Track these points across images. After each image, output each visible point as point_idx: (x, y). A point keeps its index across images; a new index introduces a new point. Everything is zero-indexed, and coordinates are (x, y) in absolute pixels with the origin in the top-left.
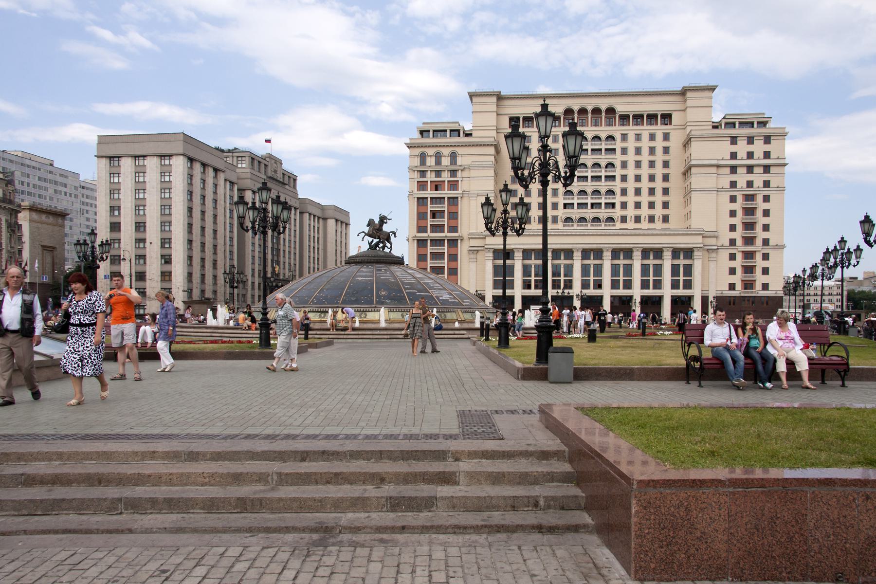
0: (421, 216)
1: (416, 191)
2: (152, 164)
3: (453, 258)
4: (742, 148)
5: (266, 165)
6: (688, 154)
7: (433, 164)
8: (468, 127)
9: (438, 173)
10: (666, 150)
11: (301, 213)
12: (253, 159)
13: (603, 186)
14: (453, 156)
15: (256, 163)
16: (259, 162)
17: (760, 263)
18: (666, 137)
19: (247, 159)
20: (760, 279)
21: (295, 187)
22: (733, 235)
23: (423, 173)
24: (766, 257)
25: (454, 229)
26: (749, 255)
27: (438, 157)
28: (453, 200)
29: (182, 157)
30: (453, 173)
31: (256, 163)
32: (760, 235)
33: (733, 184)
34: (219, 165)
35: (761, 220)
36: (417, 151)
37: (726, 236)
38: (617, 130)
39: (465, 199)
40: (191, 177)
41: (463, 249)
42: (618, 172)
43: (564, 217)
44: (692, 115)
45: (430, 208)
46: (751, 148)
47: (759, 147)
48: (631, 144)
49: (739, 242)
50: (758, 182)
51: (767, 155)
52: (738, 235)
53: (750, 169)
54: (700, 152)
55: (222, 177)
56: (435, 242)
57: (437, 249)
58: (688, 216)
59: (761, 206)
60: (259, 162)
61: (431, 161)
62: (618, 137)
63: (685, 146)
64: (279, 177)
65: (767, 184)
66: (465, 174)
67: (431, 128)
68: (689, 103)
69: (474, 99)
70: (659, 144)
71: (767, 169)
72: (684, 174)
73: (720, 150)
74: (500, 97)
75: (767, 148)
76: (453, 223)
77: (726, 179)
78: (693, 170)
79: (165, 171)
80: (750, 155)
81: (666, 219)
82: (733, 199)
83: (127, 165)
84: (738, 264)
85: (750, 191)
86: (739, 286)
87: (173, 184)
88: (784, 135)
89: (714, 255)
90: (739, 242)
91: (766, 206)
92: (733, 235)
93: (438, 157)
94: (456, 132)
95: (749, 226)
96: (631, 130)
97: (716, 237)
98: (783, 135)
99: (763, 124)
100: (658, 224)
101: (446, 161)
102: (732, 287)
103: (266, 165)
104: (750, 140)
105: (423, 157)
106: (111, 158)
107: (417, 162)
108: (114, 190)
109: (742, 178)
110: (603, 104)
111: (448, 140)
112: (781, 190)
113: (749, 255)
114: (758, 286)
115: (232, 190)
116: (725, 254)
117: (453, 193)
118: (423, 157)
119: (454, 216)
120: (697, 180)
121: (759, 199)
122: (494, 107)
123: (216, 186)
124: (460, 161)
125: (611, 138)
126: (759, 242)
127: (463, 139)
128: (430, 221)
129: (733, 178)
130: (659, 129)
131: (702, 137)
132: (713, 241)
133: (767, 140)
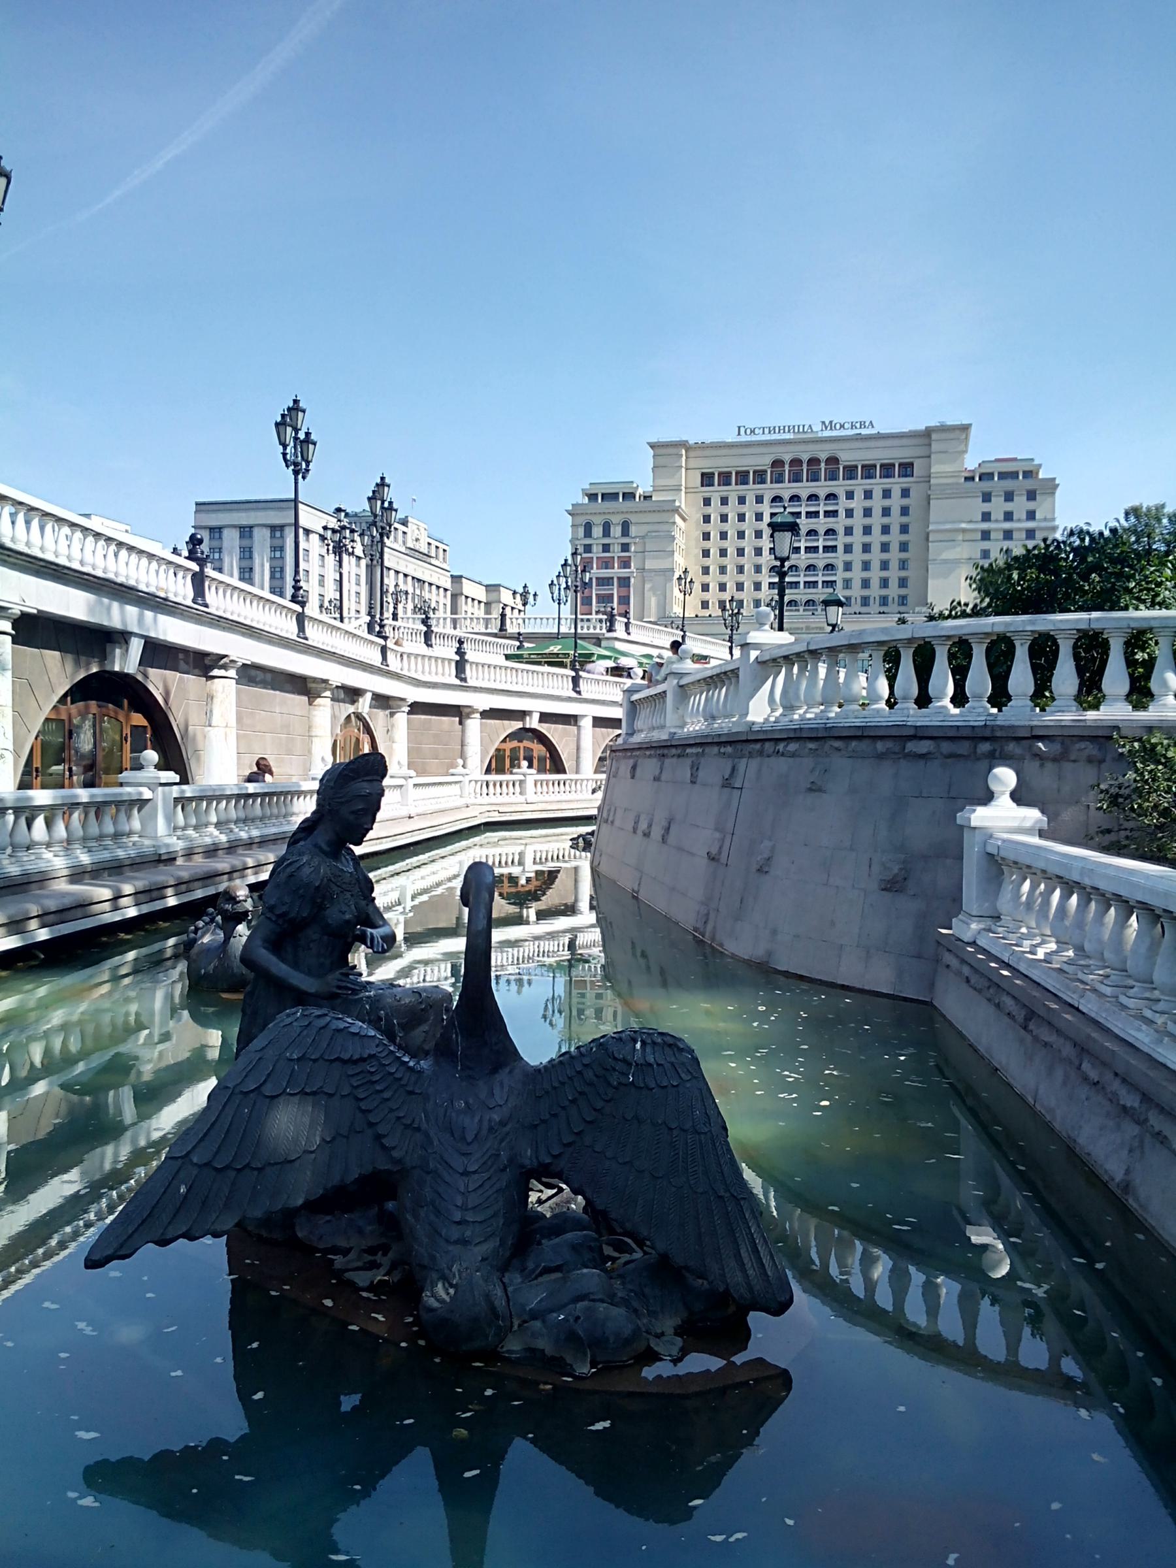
2: (261, 538)
4: (998, 506)
7: (601, 535)
9: (606, 548)
13: (821, 559)
14: (626, 527)
18: (905, 493)
27: (607, 528)
28: (625, 582)
36: (582, 520)
38: (840, 486)
42: (841, 541)
46: (1009, 506)
47: (1020, 505)
67: (599, 491)
68: (934, 447)
70: (896, 502)
80: (1008, 516)
93: (607, 528)
94: (629, 496)
96: (859, 485)
99: (1028, 474)
101: (616, 531)
103: (404, 533)
104: (1009, 497)
105: (588, 528)
107: (581, 531)
117: (624, 572)
118: (588, 528)
124: (633, 530)
130: (896, 484)
133: (1031, 496)
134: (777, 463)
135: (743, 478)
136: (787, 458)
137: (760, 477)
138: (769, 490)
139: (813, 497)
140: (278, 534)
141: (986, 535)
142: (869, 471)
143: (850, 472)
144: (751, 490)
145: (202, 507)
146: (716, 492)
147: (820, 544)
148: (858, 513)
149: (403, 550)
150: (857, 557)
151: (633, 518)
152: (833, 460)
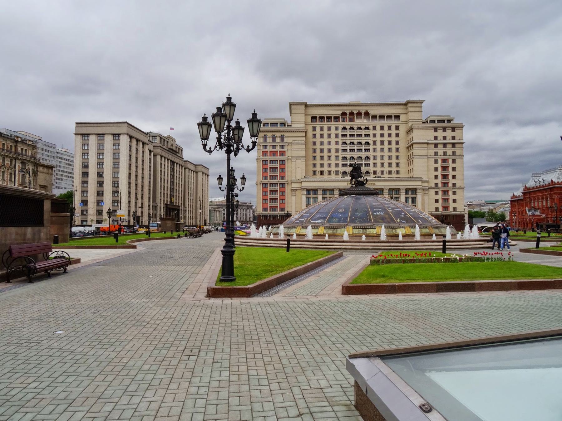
0: (265, 170)
1: (261, 157)
2: (108, 139)
3: (283, 193)
4: (440, 134)
5: (168, 142)
6: (410, 136)
8: (289, 122)
9: (274, 146)
10: (397, 135)
11: (185, 169)
12: (161, 138)
14: (282, 138)
15: (163, 140)
16: (164, 140)
17: (451, 196)
18: (397, 128)
19: (158, 138)
20: (452, 205)
21: (182, 154)
22: (436, 181)
23: (265, 146)
24: (454, 193)
25: (282, 177)
26: (445, 192)
29: (126, 135)
30: (282, 146)
31: (163, 140)
32: (451, 181)
33: (436, 153)
34: (145, 140)
35: (451, 173)
37: (433, 182)
39: (289, 161)
40: (130, 146)
41: (288, 189)
42: (371, 147)
43: (342, 171)
44: (412, 116)
45: (269, 165)
48: (378, 132)
49: (440, 185)
51: (454, 138)
52: (439, 181)
53: (445, 145)
54: (418, 136)
55: (146, 147)
56: (272, 184)
57: (273, 189)
58: (411, 171)
59: (451, 165)
60: (164, 140)
61: (269, 140)
62: (371, 128)
63: (408, 133)
64: (174, 148)
65: (454, 153)
66: (289, 147)
68: (410, 109)
69: (292, 106)
70: (393, 132)
71: (454, 145)
72: (408, 148)
73: (429, 135)
74: (306, 105)
75: (453, 134)
76: (282, 174)
77: (432, 152)
78: (414, 146)
79: (116, 144)
80: (445, 138)
81: (398, 172)
82: (436, 162)
83: (93, 140)
84: (440, 197)
86: (440, 209)
87: (121, 150)
88: (462, 127)
89: (427, 192)
90: (440, 185)
91: (454, 165)
92: (436, 181)
94: (283, 124)
95: (445, 176)
96: (378, 123)
97: (428, 182)
98: (461, 127)
100: (394, 175)
101: (278, 140)
102: (437, 209)
104: (444, 130)
106: (83, 135)
108: (85, 153)
110: (363, 110)
111: (279, 128)
112: (462, 157)
113: (445, 192)
114: (451, 209)
115: (150, 155)
116: (432, 192)
119: (283, 170)
120: (417, 151)
121: (450, 161)
122: (303, 111)
123: (143, 152)
126: (451, 185)
127: (286, 128)
128: (269, 173)
129: (436, 150)
130: (393, 123)
131: (419, 128)
132: (426, 185)
133: (453, 130)
134: (344, 114)
135: (329, 118)
136: (348, 112)
137: (336, 118)
138: (341, 125)
139: (352, 128)
140: (117, 138)
141: (436, 145)
142: (382, 117)
143: (374, 117)
144: (333, 124)
145: (80, 125)
146: (318, 125)
147: (363, 148)
148: (378, 135)
149: (167, 149)
150: (378, 154)
152: (367, 114)
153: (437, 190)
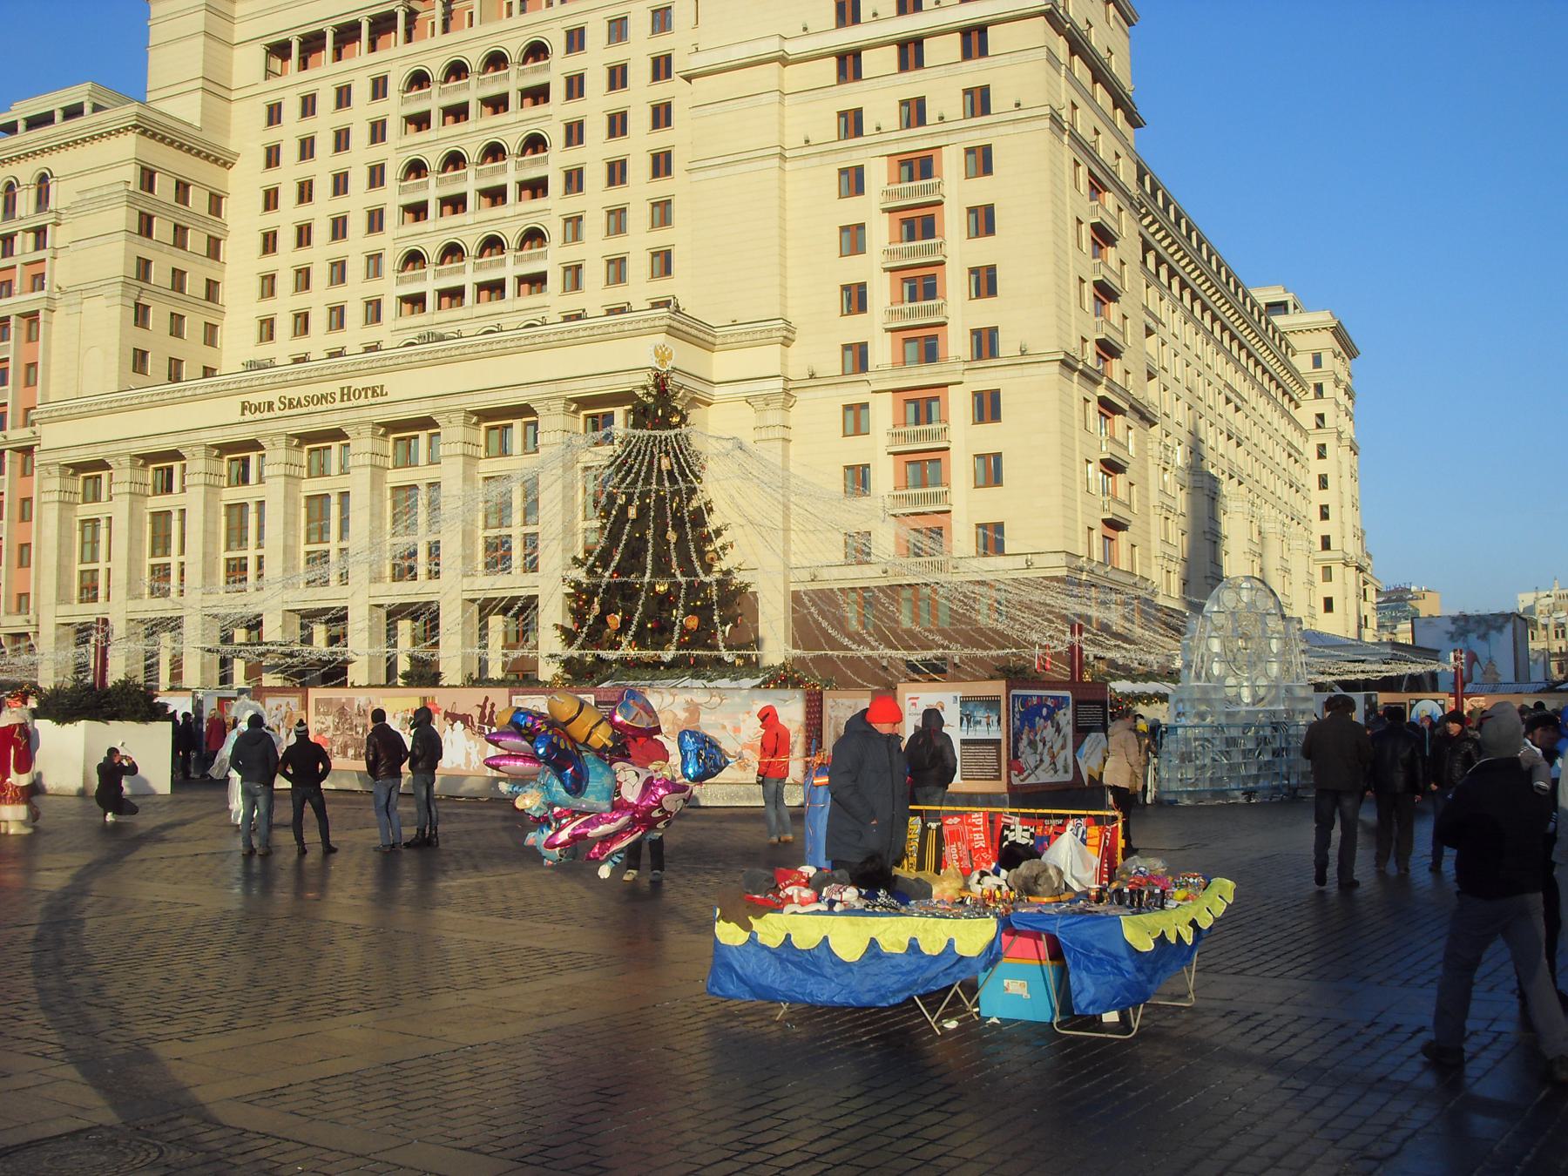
20: (967, 504)
33: (852, 123)
50: (945, 99)
85: (916, 141)
90: (882, 352)
102: (859, 549)
109: (880, 92)
114: (962, 539)
125: (537, 51)
144: (360, 65)
151: (55, 163)
153: (857, 394)
